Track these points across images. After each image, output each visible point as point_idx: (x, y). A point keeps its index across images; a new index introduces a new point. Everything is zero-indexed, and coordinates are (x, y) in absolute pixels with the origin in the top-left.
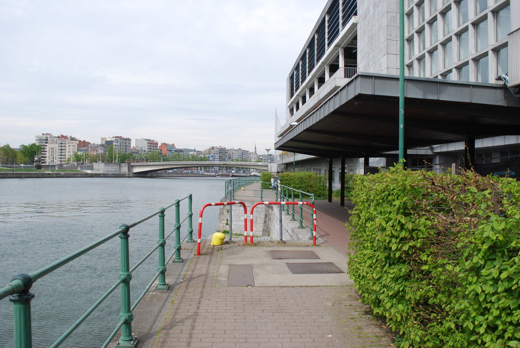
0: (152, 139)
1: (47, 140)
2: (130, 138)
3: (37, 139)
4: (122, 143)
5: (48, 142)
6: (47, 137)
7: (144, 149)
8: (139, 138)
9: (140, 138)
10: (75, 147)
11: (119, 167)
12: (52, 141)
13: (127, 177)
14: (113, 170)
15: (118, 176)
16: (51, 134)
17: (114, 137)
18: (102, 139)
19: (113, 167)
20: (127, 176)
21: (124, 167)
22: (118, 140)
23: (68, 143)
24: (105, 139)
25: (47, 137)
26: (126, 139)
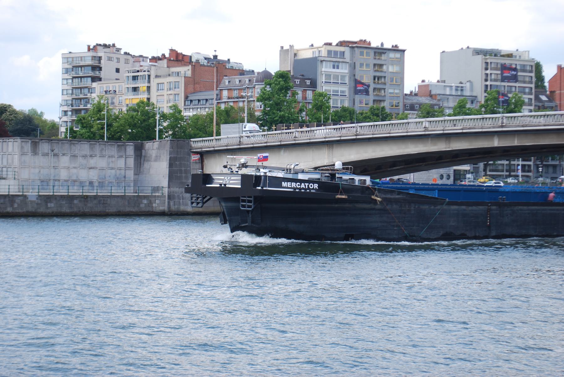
0: (506, 46)
1: (97, 68)
2: (401, 48)
3: (67, 66)
4: (361, 65)
5: (103, 74)
6: (100, 58)
7: (472, 89)
8: (453, 46)
9: (457, 48)
10: (177, 91)
11: (131, 162)
12: (118, 70)
13: (162, 214)
14: (93, 175)
15: (90, 207)
16: (114, 45)
17: (330, 44)
18: (283, 52)
19: (92, 162)
20: (165, 208)
21: (157, 159)
22: (343, 53)
23: (157, 76)
24: (291, 56)
25: (100, 58)
26: (380, 51)
